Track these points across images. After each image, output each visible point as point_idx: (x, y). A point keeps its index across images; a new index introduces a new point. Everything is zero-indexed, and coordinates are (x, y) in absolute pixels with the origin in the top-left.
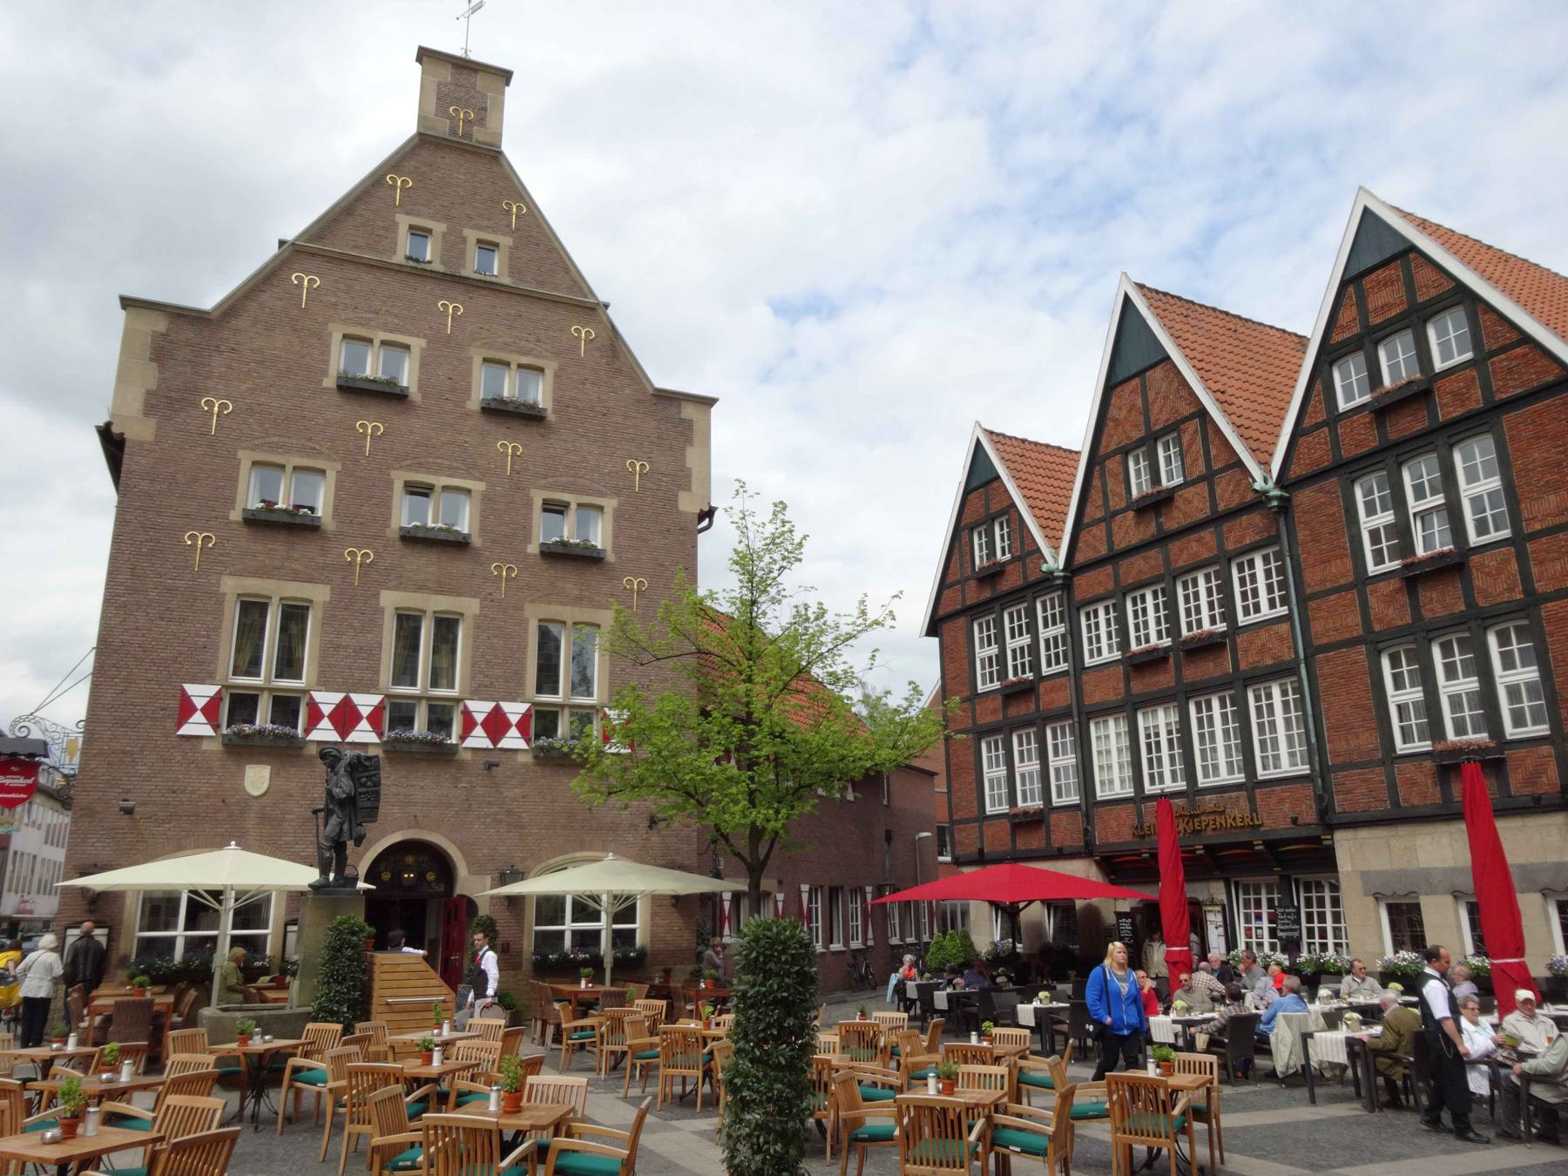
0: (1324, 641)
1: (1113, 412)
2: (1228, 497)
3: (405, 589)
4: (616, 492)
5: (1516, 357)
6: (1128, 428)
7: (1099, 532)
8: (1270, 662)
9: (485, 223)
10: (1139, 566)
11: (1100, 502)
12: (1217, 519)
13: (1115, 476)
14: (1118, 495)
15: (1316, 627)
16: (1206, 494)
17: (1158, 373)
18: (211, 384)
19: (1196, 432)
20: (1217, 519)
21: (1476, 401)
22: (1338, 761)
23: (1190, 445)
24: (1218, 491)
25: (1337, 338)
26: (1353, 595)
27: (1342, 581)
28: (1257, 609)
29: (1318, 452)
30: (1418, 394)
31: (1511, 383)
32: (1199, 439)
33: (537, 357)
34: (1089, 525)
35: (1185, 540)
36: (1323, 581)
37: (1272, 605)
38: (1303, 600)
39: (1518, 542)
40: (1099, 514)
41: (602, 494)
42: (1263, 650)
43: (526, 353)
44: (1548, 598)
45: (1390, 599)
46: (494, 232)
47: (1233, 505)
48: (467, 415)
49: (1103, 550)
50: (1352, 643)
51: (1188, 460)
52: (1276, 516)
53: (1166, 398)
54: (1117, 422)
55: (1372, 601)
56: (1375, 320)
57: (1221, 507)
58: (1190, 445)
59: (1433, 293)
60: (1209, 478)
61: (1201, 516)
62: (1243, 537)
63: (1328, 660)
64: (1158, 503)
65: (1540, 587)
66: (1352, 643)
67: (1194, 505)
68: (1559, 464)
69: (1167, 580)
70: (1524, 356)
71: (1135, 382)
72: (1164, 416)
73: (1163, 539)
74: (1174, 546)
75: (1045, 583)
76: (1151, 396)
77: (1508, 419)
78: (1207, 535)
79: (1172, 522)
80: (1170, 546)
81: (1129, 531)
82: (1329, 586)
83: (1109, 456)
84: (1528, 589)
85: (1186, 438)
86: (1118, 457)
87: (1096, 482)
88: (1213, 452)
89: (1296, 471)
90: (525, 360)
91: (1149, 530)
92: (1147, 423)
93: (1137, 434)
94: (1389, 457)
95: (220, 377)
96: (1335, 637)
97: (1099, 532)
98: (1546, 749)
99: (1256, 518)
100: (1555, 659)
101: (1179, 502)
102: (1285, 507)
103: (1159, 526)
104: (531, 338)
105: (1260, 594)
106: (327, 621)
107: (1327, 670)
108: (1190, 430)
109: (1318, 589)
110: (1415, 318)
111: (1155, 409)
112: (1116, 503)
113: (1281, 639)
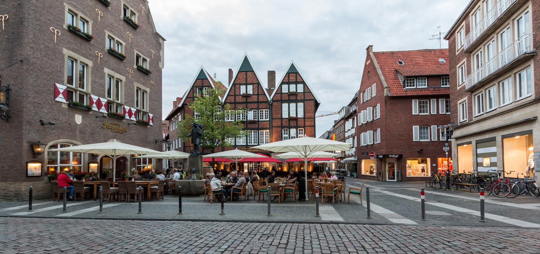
2: (261, 99)
3: (110, 69)
4: (149, 58)
7: (233, 98)
12: (258, 102)
15: (273, 123)
17: (249, 73)
21: (303, 98)
25: (284, 81)
29: (279, 97)
30: (295, 94)
38: (272, 119)
39: (304, 118)
45: (286, 122)
49: (233, 101)
52: (270, 105)
54: (239, 79)
56: (290, 81)
60: (258, 95)
64: (246, 96)
66: (279, 127)
67: (255, 98)
73: (246, 103)
77: (306, 102)
78: (256, 105)
79: (249, 100)
81: (239, 99)
87: (233, 88)
89: (274, 99)
91: (245, 100)
94: (289, 101)
99: (265, 104)
103: (247, 99)
105: (265, 116)
106: (93, 72)
110: (296, 83)
111: (248, 80)
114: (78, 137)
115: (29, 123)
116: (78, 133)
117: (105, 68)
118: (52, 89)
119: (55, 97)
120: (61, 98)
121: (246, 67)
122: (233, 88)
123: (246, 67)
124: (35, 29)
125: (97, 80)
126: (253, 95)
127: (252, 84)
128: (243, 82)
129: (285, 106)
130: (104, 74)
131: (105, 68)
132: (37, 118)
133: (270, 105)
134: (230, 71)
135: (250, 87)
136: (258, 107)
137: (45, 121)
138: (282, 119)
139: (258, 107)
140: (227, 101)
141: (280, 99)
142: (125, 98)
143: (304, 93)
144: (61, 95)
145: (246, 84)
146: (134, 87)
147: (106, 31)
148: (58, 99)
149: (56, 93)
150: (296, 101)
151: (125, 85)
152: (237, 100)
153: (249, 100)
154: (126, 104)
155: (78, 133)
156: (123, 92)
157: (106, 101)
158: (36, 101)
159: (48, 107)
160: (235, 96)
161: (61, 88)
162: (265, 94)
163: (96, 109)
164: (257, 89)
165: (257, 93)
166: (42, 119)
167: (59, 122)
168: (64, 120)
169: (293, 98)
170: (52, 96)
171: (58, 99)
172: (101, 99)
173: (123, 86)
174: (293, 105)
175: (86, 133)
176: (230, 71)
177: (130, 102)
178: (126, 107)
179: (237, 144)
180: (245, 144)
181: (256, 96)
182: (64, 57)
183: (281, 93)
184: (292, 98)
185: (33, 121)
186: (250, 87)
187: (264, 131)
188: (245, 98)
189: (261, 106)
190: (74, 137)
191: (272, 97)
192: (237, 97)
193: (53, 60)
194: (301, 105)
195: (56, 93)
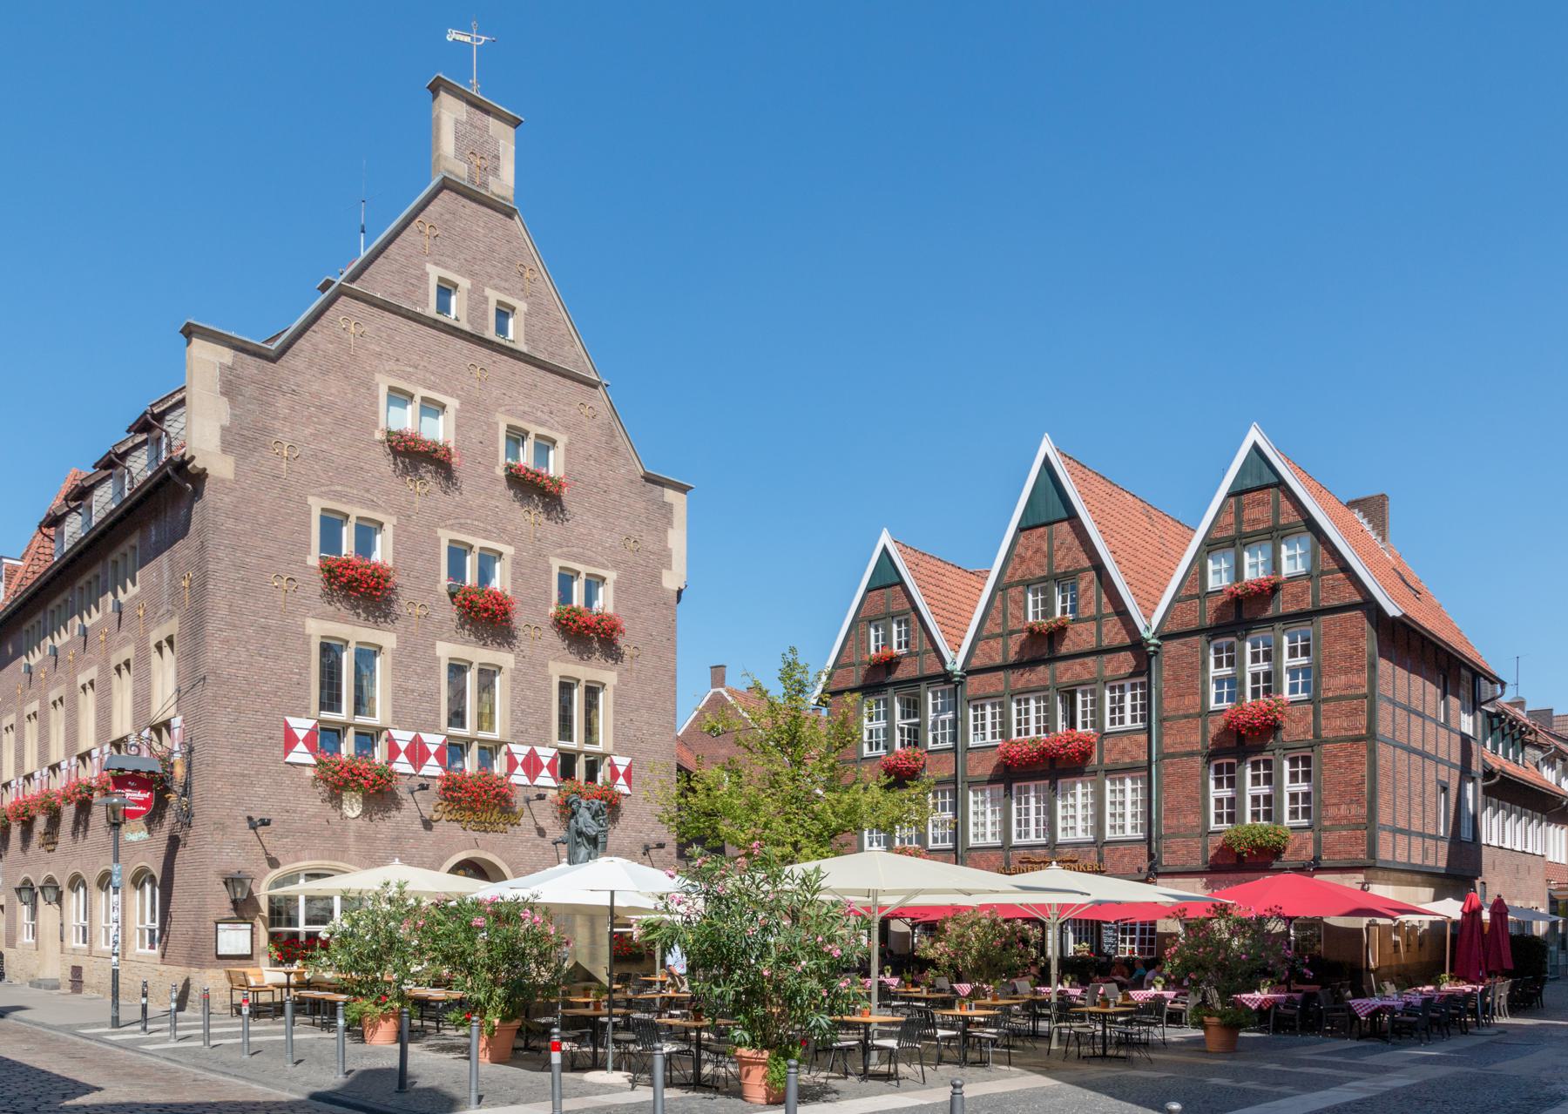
1: (1019, 549)
6: (1032, 565)
9: (503, 284)
13: (1016, 602)
15: (1167, 740)
18: (277, 424)
24: (1104, 630)
28: (1122, 721)
33: (551, 428)
36: (1177, 709)
37: (1134, 719)
38: (1161, 721)
40: (998, 630)
41: (605, 567)
42: (1123, 752)
43: (542, 424)
44: (1327, 741)
46: (511, 295)
47: (1116, 644)
48: (495, 480)
50: (1191, 754)
53: (1069, 549)
54: (1022, 559)
57: (1105, 643)
61: (1087, 647)
66: (1191, 754)
68: (1351, 657)
72: (1066, 563)
75: (946, 677)
76: (1056, 543)
78: (1089, 661)
83: (1010, 585)
84: (1316, 736)
85: (1082, 585)
87: (997, 603)
90: (543, 431)
92: (1050, 564)
93: (1039, 573)
95: (285, 419)
96: (1180, 749)
97: (996, 644)
98: (1308, 834)
101: (1070, 633)
104: (546, 409)
111: (1060, 554)
113: (1139, 746)
114: (352, 852)
115: (221, 827)
116: (351, 840)
117: (439, 644)
118: (280, 734)
119: (287, 751)
120: (301, 754)
124: (234, 591)
125: (411, 684)
130: (438, 659)
131: (439, 644)
132: (241, 814)
137: (257, 817)
142: (514, 720)
144: (301, 747)
146: (548, 678)
147: (441, 532)
148: (292, 758)
149: (290, 740)
151: (514, 680)
154: (518, 737)
155: (351, 840)
156: (508, 702)
157: (440, 739)
158: (237, 769)
159: (268, 781)
161: (302, 726)
163: (409, 769)
166: (252, 815)
167: (296, 816)
168: (312, 811)
170: (279, 751)
171: (292, 758)
172: (425, 737)
173: (508, 684)
175: (376, 839)
177: (532, 730)
178: (514, 748)
182: (308, 644)
185: (228, 822)
190: (340, 852)
191: (1156, 620)
193: (277, 658)
195: (290, 740)
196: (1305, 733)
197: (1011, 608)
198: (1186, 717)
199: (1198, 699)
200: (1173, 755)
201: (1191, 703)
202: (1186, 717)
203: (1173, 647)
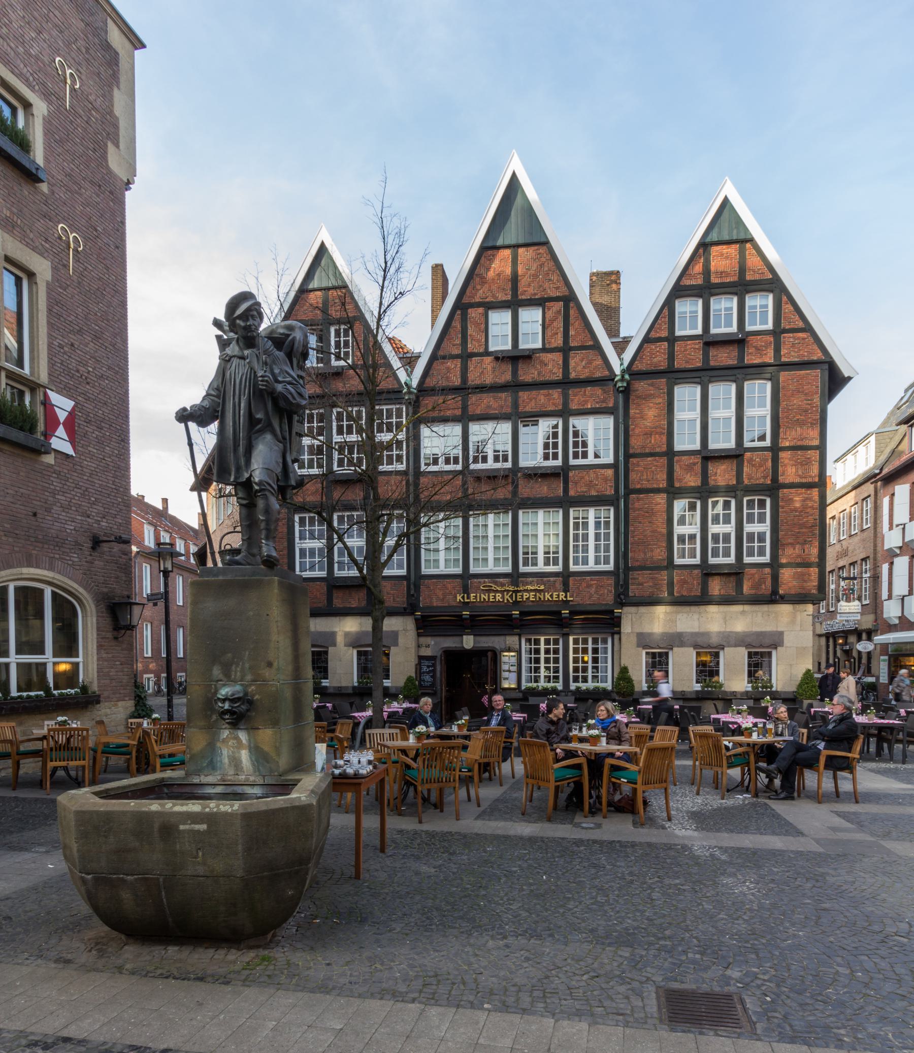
0: (638, 486)
2: (579, 367)
5: (799, 338)
6: (494, 287)
7: (455, 366)
8: (594, 493)
10: (487, 402)
11: (458, 341)
12: (566, 383)
13: (477, 325)
14: (479, 341)
15: (633, 476)
16: (561, 362)
19: (559, 312)
20: (566, 383)
22: (637, 564)
23: (552, 321)
24: (572, 363)
26: (664, 460)
27: (658, 450)
31: (792, 353)
32: (561, 318)
34: (444, 358)
35: (534, 393)
38: (628, 456)
40: (457, 351)
42: (590, 485)
50: (658, 491)
51: (549, 333)
52: (621, 396)
55: (677, 467)
57: (573, 375)
58: (552, 321)
59: (757, 277)
60: (566, 350)
62: (586, 402)
63: (638, 500)
64: (516, 358)
65: (781, 479)
67: (552, 367)
69: (522, 417)
70: (804, 339)
71: (507, 252)
72: (531, 290)
73: (515, 386)
74: (524, 395)
75: (395, 394)
78: (556, 394)
79: (528, 374)
80: (521, 394)
81: (484, 372)
82: (647, 451)
85: (549, 314)
86: (481, 310)
87: (457, 324)
88: (572, 333)
91: (507, 377)
99: (598, 391)
100: (782, 521)
102: (626, 392)
103: (515, 373)
107: (637, 505)
108: (554, 309)
109: (639, 451)
112: (471, 347)
113: (606, 480)
121: (514, 224)
122: (457, 324)
123: (514, 224)
126: (544, 350)
127: (539, 302)
128: (501, 297)
129: (687, 396)
133: (621, 396)
134: (439, 272)
135: (532, 318)
136: (566, 403)
138: (670, 454)
139: (566, 403)
140: (430, 382)
141: (663, 366)
143: (777, 332)
145: (514, 304)
150: (740, 373)
152: (474, 378)
153: (528, 374)
160: (466, 357)
162: (597, 347)
164: (559, 324)
165: (559, 341)
169: (724, 357)
174: (723, 393)
176: (439, 272)
179: (473, 569)
180: (508, 569)
181: (558, 357)
183: (672, 339)
184: (725, 360)
186: (532, 318)
187: (592, 513)
188: (508, 368)
189: (577, 398)
192: (473, 363)
194: (759, 392)
196: (765, 477)
197: (471, 331)
198: (652, 455)
199: (664, 438)
200: (640, 491)
201: (658, 443)
202: (652, 455)
203: (641, 386)
